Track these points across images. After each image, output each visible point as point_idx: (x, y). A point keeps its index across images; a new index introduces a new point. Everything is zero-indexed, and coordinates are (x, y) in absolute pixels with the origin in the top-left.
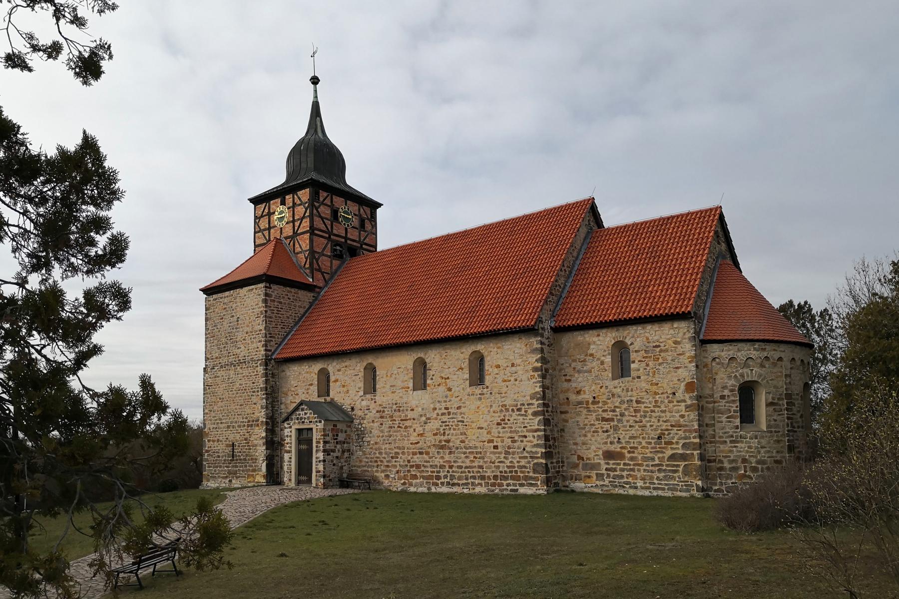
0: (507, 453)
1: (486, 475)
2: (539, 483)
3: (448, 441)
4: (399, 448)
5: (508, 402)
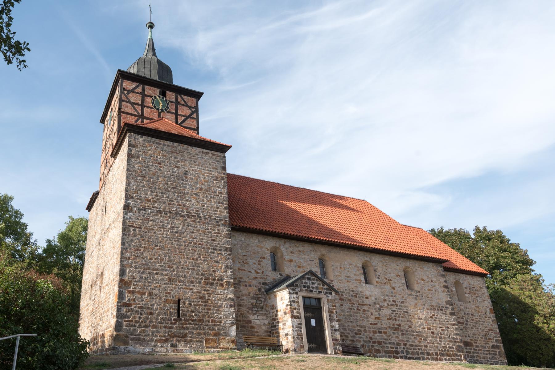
0: (440, 337)
1: (431, 352)
2: (462, 358)
3: (400, 325)
4: (359, 326)
5: (434, 304)
